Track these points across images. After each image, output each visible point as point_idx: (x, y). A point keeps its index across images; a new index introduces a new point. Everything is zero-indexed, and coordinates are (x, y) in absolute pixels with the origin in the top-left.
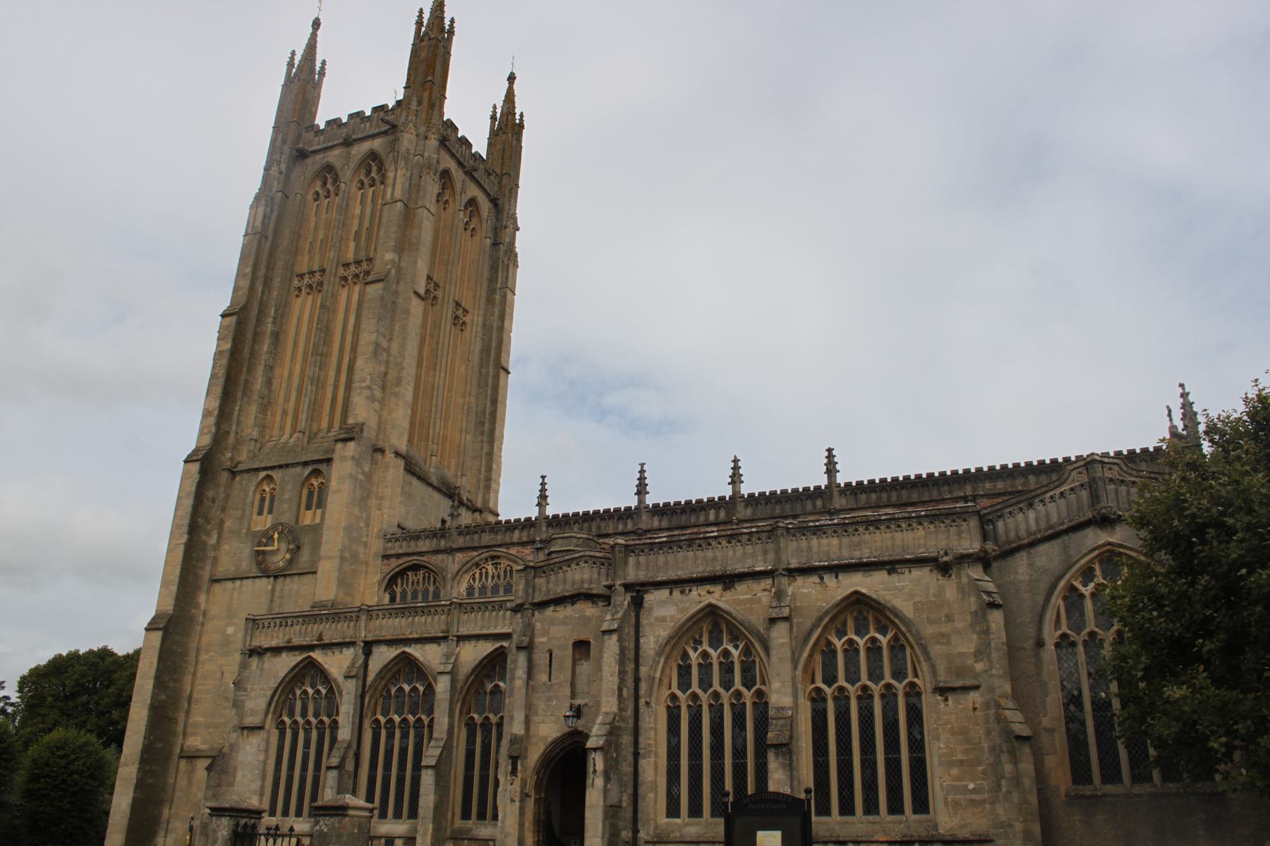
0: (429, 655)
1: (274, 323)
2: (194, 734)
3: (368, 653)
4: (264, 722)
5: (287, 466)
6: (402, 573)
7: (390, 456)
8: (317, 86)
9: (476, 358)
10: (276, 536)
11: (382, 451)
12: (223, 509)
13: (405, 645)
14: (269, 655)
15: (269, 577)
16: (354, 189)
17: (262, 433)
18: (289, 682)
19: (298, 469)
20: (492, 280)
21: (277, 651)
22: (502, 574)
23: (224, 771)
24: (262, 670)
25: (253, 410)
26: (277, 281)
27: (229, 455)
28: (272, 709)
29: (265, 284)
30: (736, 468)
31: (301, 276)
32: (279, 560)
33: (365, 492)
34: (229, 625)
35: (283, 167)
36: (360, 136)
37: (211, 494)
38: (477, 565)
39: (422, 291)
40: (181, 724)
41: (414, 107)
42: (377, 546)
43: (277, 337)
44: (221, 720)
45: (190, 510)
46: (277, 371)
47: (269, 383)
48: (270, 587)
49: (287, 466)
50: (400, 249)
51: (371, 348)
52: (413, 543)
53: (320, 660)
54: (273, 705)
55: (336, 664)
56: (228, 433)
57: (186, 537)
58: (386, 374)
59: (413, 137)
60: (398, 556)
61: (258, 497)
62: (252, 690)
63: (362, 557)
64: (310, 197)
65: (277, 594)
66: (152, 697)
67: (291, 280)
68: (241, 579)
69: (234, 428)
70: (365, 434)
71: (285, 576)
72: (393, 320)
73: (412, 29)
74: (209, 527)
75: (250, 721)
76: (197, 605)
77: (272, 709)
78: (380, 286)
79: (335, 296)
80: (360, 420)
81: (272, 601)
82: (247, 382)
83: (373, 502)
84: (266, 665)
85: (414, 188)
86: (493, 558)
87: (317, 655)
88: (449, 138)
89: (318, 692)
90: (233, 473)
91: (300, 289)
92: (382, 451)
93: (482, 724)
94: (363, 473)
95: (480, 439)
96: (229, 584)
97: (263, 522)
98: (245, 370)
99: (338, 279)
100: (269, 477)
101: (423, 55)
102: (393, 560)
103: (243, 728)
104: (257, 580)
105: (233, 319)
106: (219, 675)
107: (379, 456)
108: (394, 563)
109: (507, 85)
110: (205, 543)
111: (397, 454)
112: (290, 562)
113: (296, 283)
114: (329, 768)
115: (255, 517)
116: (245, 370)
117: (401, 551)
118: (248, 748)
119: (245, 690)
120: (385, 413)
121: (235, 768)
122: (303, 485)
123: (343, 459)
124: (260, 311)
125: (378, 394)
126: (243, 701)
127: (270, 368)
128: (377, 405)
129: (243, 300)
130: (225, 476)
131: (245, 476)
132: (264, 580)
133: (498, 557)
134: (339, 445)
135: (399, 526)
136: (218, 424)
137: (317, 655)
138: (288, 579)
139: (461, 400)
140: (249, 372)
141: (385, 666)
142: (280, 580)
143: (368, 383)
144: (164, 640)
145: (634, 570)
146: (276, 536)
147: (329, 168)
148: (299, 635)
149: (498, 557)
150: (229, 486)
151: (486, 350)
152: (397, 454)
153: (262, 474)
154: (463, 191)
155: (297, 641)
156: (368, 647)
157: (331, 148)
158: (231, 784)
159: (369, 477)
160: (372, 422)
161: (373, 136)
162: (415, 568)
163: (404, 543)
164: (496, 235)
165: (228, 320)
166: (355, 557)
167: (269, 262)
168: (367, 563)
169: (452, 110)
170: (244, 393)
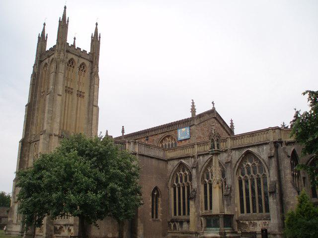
8: (46, 41)
12: (29, 152)
20: (91, 83)
23: (12, 211)
30: (123, 128)
37: (26, 148)
39: (61, 94)
43: (38, 109)
47: (37, 120)
78: (48, 95)
90: (30, 143)
107: (51, 137)
109: (95, 26)
111: (55, 136)
120: (52, 126)
125: (50, 122)
128: (50, 125)
147: (46, 64)
150: (30, 146)
154: (78, 62)
169: (70, 41)
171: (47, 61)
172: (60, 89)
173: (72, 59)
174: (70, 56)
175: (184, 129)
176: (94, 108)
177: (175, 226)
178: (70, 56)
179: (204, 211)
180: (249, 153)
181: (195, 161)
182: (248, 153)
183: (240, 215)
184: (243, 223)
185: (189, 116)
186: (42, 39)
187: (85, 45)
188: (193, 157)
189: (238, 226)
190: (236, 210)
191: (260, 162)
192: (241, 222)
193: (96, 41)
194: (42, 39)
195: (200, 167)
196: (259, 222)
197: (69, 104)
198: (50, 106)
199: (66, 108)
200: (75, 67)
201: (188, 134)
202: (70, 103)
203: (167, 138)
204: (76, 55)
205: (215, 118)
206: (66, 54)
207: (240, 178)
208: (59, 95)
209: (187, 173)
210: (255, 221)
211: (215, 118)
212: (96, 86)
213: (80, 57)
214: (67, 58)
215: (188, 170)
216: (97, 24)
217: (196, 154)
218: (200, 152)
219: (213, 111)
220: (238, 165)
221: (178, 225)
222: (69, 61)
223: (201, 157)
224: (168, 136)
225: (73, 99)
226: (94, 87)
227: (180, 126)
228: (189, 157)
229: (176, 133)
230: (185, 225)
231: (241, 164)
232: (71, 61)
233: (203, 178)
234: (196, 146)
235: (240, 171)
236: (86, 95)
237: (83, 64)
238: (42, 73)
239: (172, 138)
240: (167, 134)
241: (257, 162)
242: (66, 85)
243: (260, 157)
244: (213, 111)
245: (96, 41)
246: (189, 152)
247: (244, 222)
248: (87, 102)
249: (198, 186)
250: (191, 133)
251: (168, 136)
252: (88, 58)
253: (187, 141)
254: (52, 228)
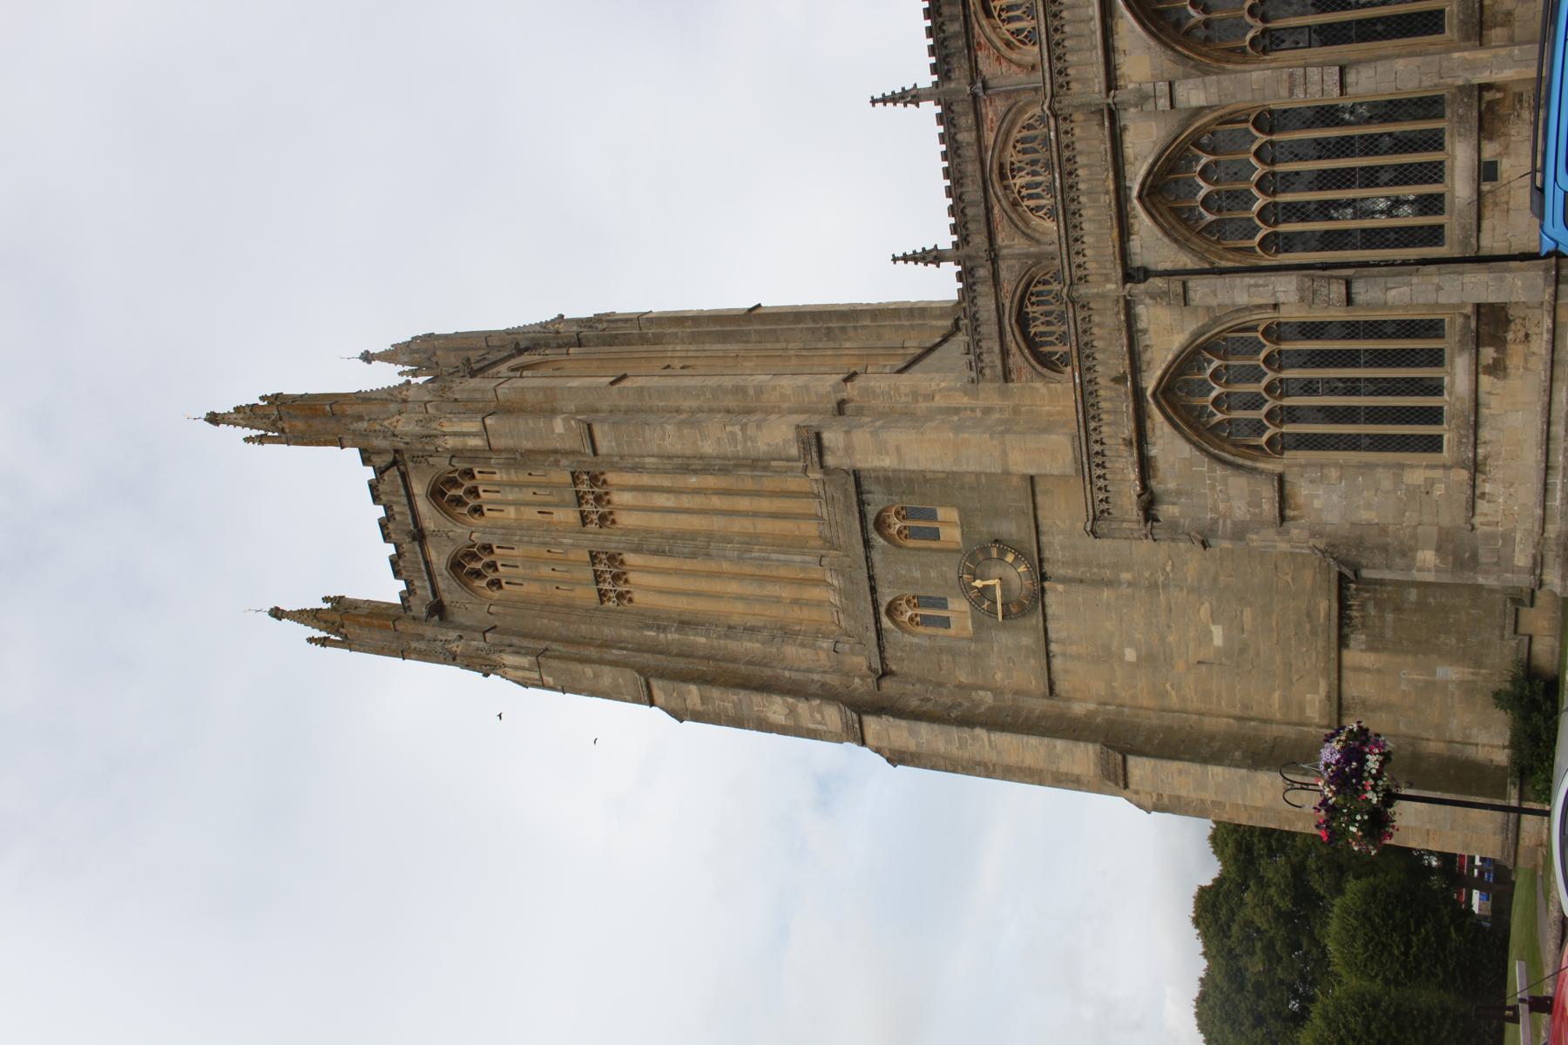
0: (1144, 142)
1: (665, 629)
2: (1302, 708)
3: (1146, 274)
4: (1270, 474)
5: (871, 578)
7: (851, 390)
9: (733, 347)
10: (978, 583)
13: (1128, 199)
14: (1153, 483)
15: (1043, 590)
17: (825, 636)
18: (1200, 436)
19: (876, 556)
21: (1145, 467)
22: (1028, 157)
23: (1360, 543)
24: (1179, 493)
25: (791, 651)
26: (608, 632)
27: (857, 680)
28: (1248, 463)
31: (602, 595)
32: (1017, 574)
34: (1121, 657)
35: (453, 635)
36: (410, 520)
38: (1015, 204)
40: (1285, 728)
41: (364, 425)
42: (989, 395)
43: (685, 624)
44: (1278, 658)
45: (936, 727)
46: (735, 620)
48: (1060, 587)
49: (871, 578)
52: (983, 329)
53: (1159, 373)
54: (1240, 461)
55: (1166, 334)
56: (823, 685)
57: (979, 731)
58: (728, 411)
60: (1005, 354)
62: (1215, 509)
65: (1070, 572)
66: (1237, 766)
67: (610, 611)
68: (1047, 642)
69: (816, 677)
71: (1041, 561)
73: (269, 448)
74: (966, 704)
75: (1269, 508)
76: (1091, 715)
77: (1248, 463)
79: (628, 531)
80: (791, 435)
81: (1081, 581)
82: (749, 663)
84: (1172, 485)
85: (467, 407)
86: (1003, 177)
87: (1150, 383)
89: (1215, 375)
90: (886, 673)
91: (620, 596)
93: (1264, 19)
95: (851, 333)
96: (1057, 663)
97: (958, 607)
98: (731, 666)
99: (604, 530)
100: (889, 612)
101: (300, 425)
102: (1011, 361)
103: (1283, 518)
104: (1049, 611)
106: (1204, 668)
107: (849, 407)
108: (1016, 360)
110: (991, 709)
112: (1020, 554)
114: (1349, 300)
115: (952, 631)
116: (731, 666)
117: (997, 349)
118: (1317, 504)
119: (1215, 521)
121: (1353, 524)
122: (899, 547)
123: (849, 449)
126: (1235, 524)
130: (887, 684)
131: (888, 653)
132: (1050, 598)
133: (1001, 166)
134: (830, 460)
136: (807, 697)
137: (1150, 383)
138: (1047, 554)
139: (794, 361)
140: (734, 660)
141: (1166, 233)
142: (1047, 568)
143: (737, 429)
144: (1141, 753)
146: (978, 583)
147: (456, 566)
148: (1117, 428)
149: (1001, 166)
151: (724, 337)
153: (886, 622)
155: (1128, 429)
156: (1132, 274)
157: (427, 563)
158: (1383, 530)
161: (410, 496)
162: (1023, 321)
163: (984, 344)
164: (569, 345)
165: (659, 695)
170: (765, 665)
186: (343, 623)
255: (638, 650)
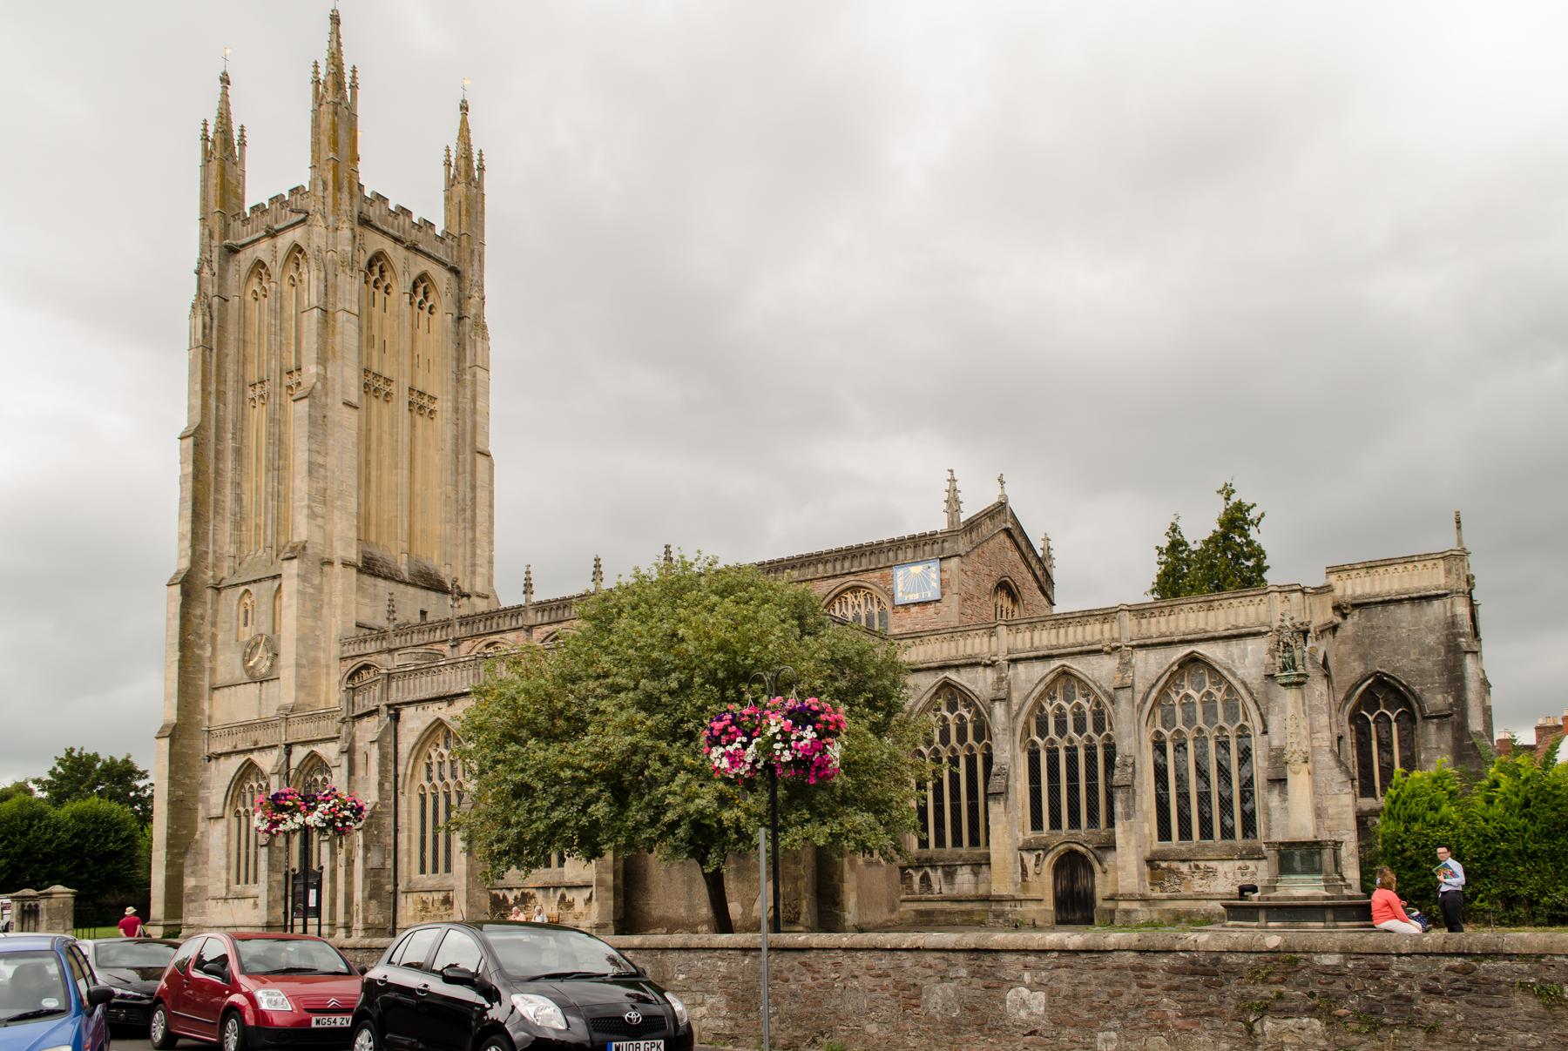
6: (357, 672)
11: (330, 563)
16: (286, 286)
17: (239, 549)
19: (268, 584)
25: (228, 527)
27: (211, 573)
29: (218, 399)
33: (313, 606)
35: (215, 266)
39: (354, 400)
42: (335, 650)
43: (238, 452)
46: (246, 486)
47: (238, 499)
50: (322, 360)
51: (305, 467)
59: (323, 231)
60: (352, 657)
61: (242, 610)
63: (323, 661)
64: (249, 298)
67: (244, 392)
70: (309, 551)
72: (325, 433)
78: (305, 402)
82: (217, 501)
83: (325, 611)
88: (369, 216)
90: (218, 590)
92: (330, 563)
94: (313, 586)
105: (190, 441)
107: (326, 568)
108: (350, 663)
111: (345, 564)
113: (250, 393)
115: (242, 628)
120: (328, 528)
124: (217, 427)
127: (237, 485)
128: (320, 521)
129: (198, 419)
130: (209, 592)
131: (229, 591)
135: (359, 625)
136: (193, 547)
140: (217, 491)
145: (395, 697)
147: (260, 264)
150: (215, 602)
152: (345, 564)
153: (242, 589)
159: (320, 589)
160: (318, 538)
166: (314, 662)
167: (218, 375)
168: (328, 666)
170: (216, 513)
171: (262, 250)
172: (347, 378)
173: (379, 256)
174: (375, 242)
175: (916, 569)
176: (480, 459)
177: (925, 879)
178: (375, 242)
179: (1030, 834)
180: (1192, 662)
181: (1000, 680)
182: (1192, 661)
183: (1157, 845)
184: (1169, 870)
185: (941, 524)
186: (223, 152)
187: (427, 202)
188: (992, 665)
189: (1153, 877)
190: (1147, 831)
191: (1230, 689)
192: (1164, 865)
193: (466, 177)
194: (223, 152)
195: (1016, 697)
196: (1223, 867)
197: (380, 441)
198: (315, 447)
199: (373, 458)
200: (394, 291)
201: (935, 585)
202: (386, 438)
203: (849, 596)
204: (397, 240)
205: (1007, 531)
206: (358, 229)
207: (1158, 734)
208: (347, 404)
209: (968, 716)
210: (1210, 864)
211: (1007, 531)
212: (480, 374)
213: (413, 248)
214: (362, 247)
215: (969, 704)
216: (464, 108)
217: (1002, 659)
218: (1018, 651)
219: (1001, 507)
220: (1154, 693)
221: (936, 876)
222: (370, 265)
223: (1021, 667)
224: (854, 589)
225: (394, 423)
226: (474, 376)
227: (901, 556)
228: (977, 664)
229: (889, 580)
230: (964, 877)
231: (1164, 693)
232: (377, 262)
233: (1027, 731)
234: (1002, 631)
235: (1158, 712)
236: (443, 406)
237: (423, 277)
238: (243, 303)
239: (869, 597)
240: (851, 581)
241: (1219, 690)
242: (364, 365)
243: (1234, 675)
244: (1001, 507)
245: (466, 177)
246: (977, 645)
247: (1174, 865)
248: (449, 432)
249: (1013, 757)
250: (944, 584)
251: (854, 589)
252: (441, 255)
253: (931, 609)
254: (486, 902)
255: (217, 420)
